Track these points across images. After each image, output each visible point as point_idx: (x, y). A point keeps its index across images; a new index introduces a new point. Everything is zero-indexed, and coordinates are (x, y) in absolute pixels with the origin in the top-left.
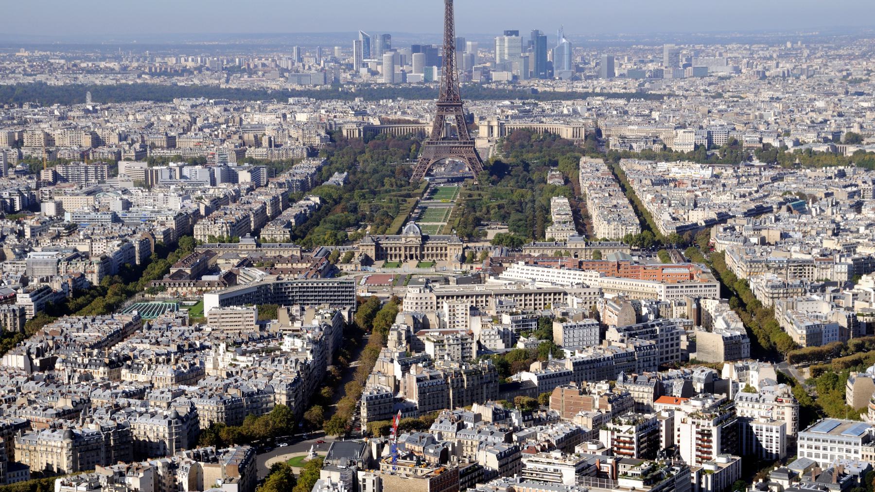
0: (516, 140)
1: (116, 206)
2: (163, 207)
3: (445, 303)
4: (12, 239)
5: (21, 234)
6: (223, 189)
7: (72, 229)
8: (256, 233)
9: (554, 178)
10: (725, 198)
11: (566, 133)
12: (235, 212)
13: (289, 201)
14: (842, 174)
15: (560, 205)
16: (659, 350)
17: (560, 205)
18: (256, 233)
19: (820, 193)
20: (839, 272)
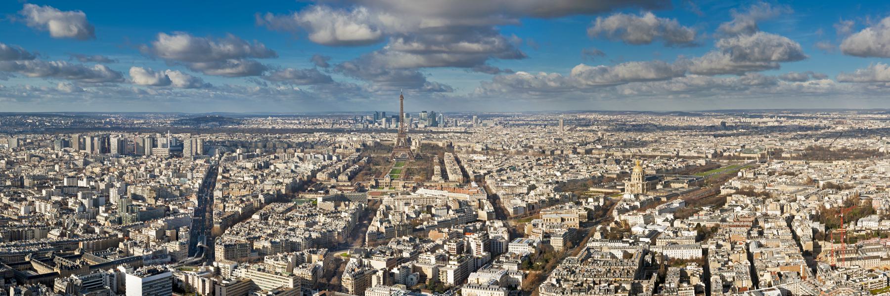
0: (424, 147)
1: (293, 167)
2: (306, 168)
3: (398, 202)
4: (260, 177)
5: (262, 175)
6: (328, 162)
7: (278, 174)
8: (336, 177)
9: (436, 160)
10: (491, 166)
11: (440, 144)
12: (330, 170)
13: (348, 166)
14: (527, 158)
15: (437, 168)
16: (466, 216)
17: (437, 168)
18: (336, 177)
19: (520, 164)
20: (525, 190)
